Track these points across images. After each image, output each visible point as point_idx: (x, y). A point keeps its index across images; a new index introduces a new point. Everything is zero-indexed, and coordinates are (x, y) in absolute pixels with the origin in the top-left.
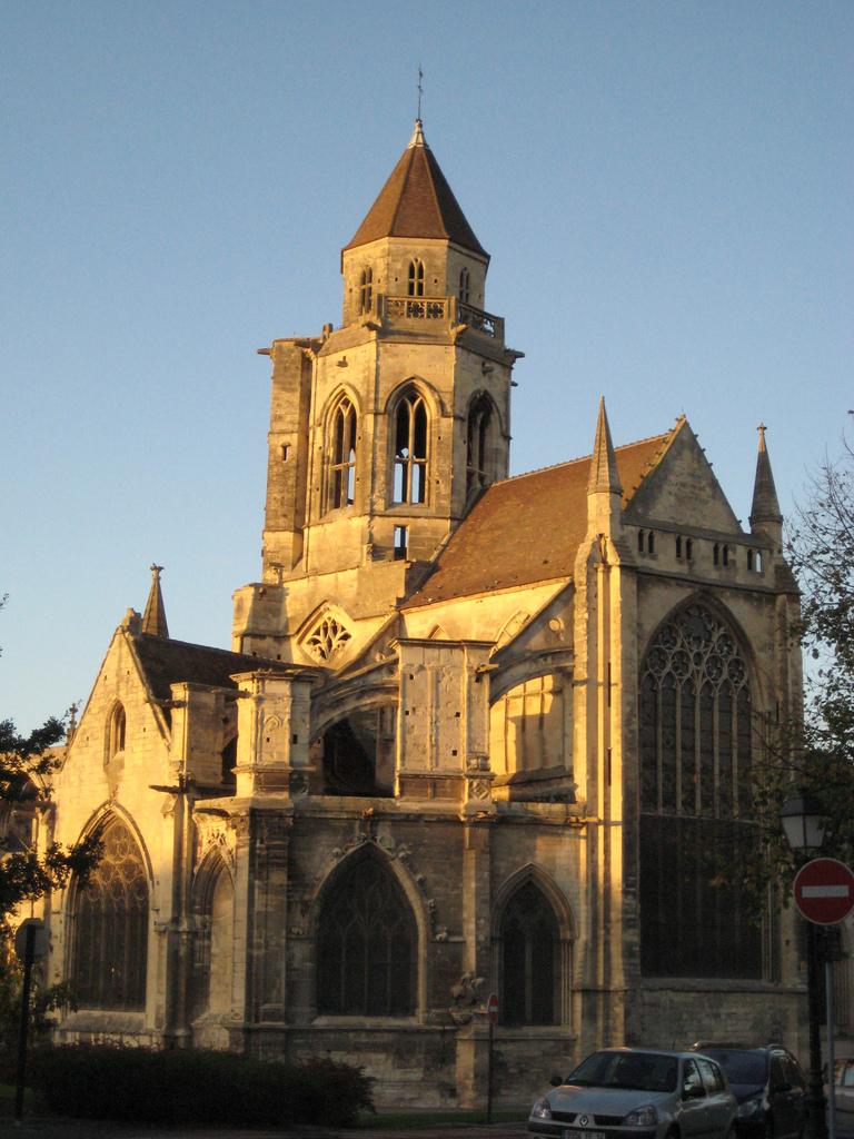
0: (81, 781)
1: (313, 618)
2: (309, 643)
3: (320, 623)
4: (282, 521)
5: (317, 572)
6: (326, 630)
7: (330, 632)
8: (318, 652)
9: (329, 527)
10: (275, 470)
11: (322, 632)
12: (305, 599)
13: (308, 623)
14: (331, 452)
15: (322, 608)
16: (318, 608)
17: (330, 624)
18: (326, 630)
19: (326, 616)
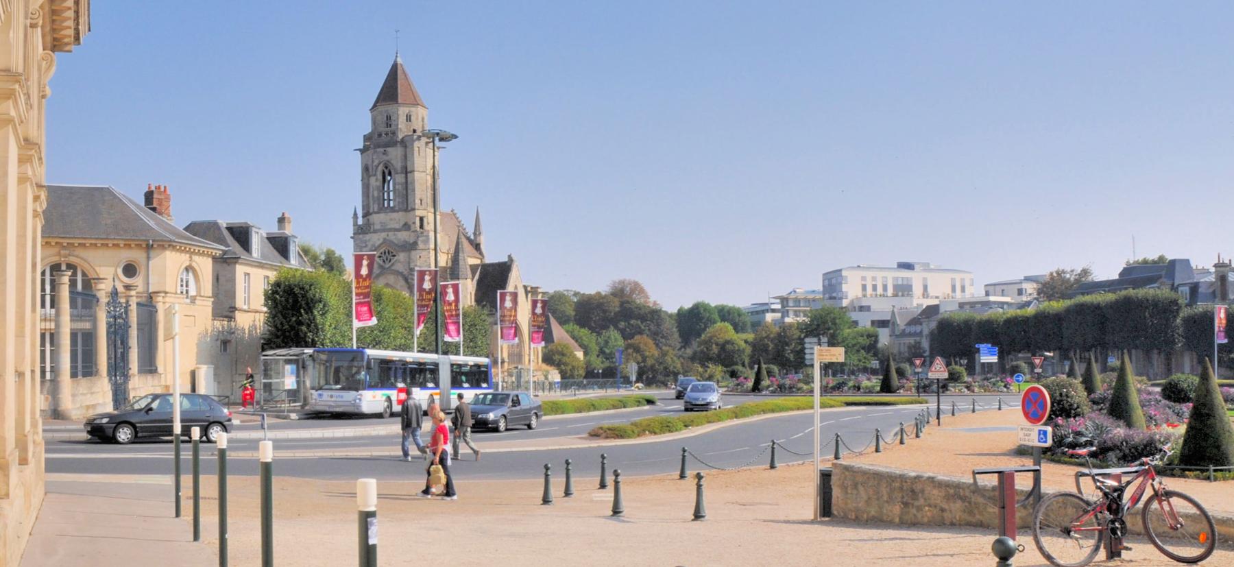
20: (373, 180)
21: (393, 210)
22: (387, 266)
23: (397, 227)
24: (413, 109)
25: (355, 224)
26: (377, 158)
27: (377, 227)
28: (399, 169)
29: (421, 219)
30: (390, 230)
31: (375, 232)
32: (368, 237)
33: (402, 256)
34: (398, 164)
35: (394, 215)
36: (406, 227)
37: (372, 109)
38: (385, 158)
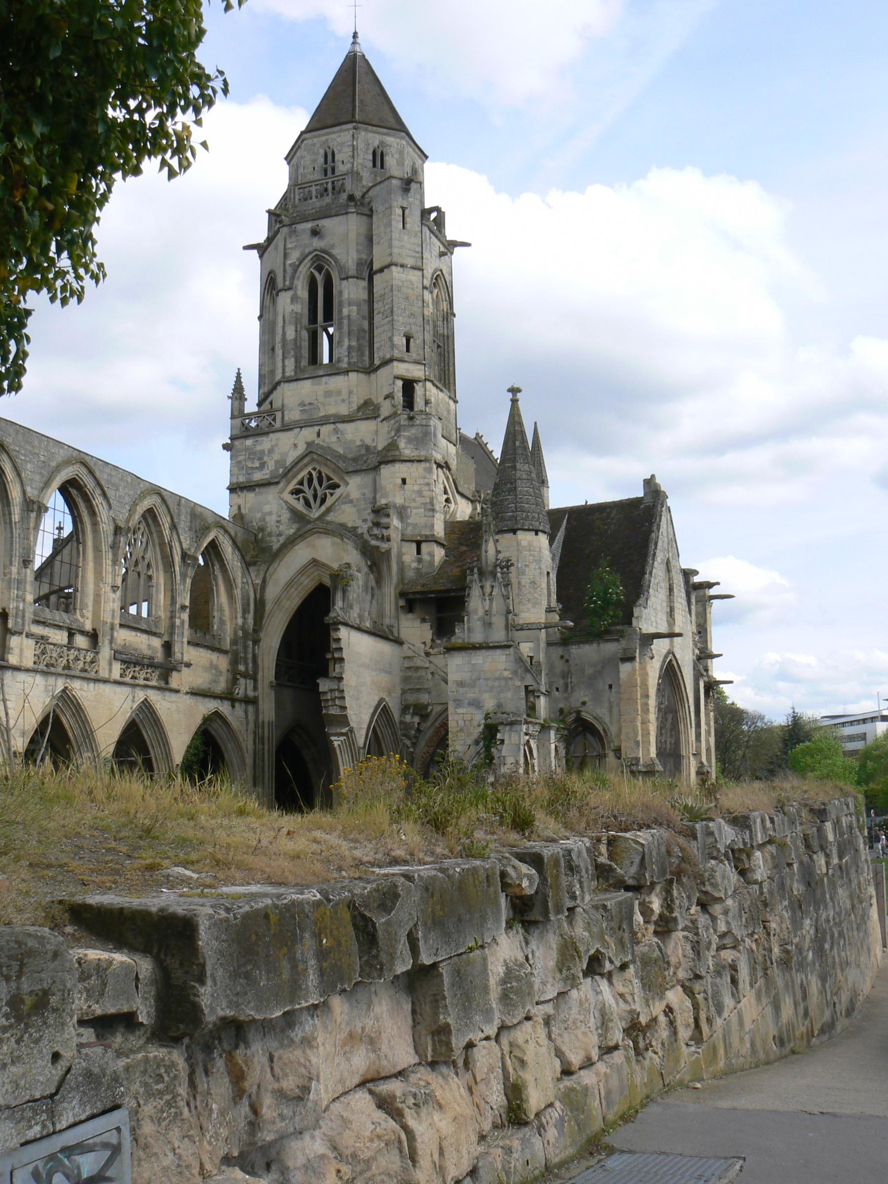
20: (284, 299)
21: (334, 370)
22: (315, 513)
23: (344, 410)
24: (389, 140)
25: (238, 413)
26: (300, 244)
27: (292, 415)
28: (352, 270)
29: (409, 386)
30: (325, 421)
31: (286, 428)
32: (265, 443)
33: (354, 487)
34: (348, 255)
35: (338, 382)
36: (368, 410)
37: (289, 158)
38: (317, 243)
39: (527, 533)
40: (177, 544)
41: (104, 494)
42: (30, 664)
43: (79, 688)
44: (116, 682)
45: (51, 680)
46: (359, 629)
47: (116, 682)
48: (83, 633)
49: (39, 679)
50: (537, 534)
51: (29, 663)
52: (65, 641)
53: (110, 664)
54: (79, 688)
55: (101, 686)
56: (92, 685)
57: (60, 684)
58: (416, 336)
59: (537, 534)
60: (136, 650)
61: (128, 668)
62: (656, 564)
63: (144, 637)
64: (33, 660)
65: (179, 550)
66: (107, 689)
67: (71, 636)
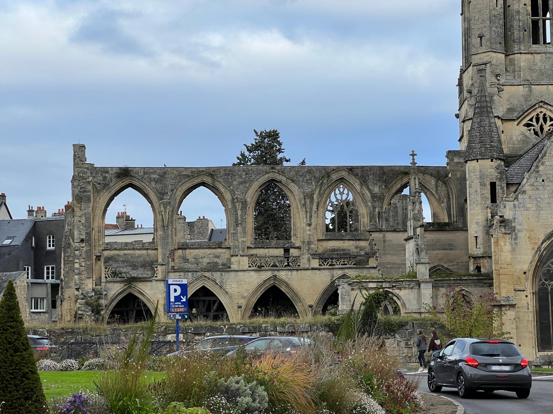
0: (539, 208)
1: (530, 111)
2: (524, 125)
3: (534, 114)
4: (498, 46)
5: (529, 84)
6: (538, 120)
7: (541, 120)
8: (532, 132)
9: (538, 57)
10: (493, 12)
11: (534, 120)
12: (522, 99)
13: (526, 114)
14: (529, 8)
15: (537, 106)
16: (535, 105)
17: (541, 116)
18: (538, 120)
19: (538, 110)
39: (473, 161)
40: (367, 192)
41: (293, 181)
42: (246, 267)
43: (283, 275)
44: (313, 269)
45: (261, 273)
46: (395, 231)
47: (313, 269)
48: (295, 248)
49: (252, 273)
50: (478, 162)
51: (246, 267)
52: (283, 252)
53: (309, 260)
54: (283, 275)
55: (303, 271)
56: (295, 273)
57: (268, 275)
58: (485, 35)
59: (478, 162)
60: (343, 250)
61: (325, 261)
62: (541, 168)
63: (351, 242)
64: (248, 265)
65: (369, 195)
66: (308, 272)
67: (287, 251)
